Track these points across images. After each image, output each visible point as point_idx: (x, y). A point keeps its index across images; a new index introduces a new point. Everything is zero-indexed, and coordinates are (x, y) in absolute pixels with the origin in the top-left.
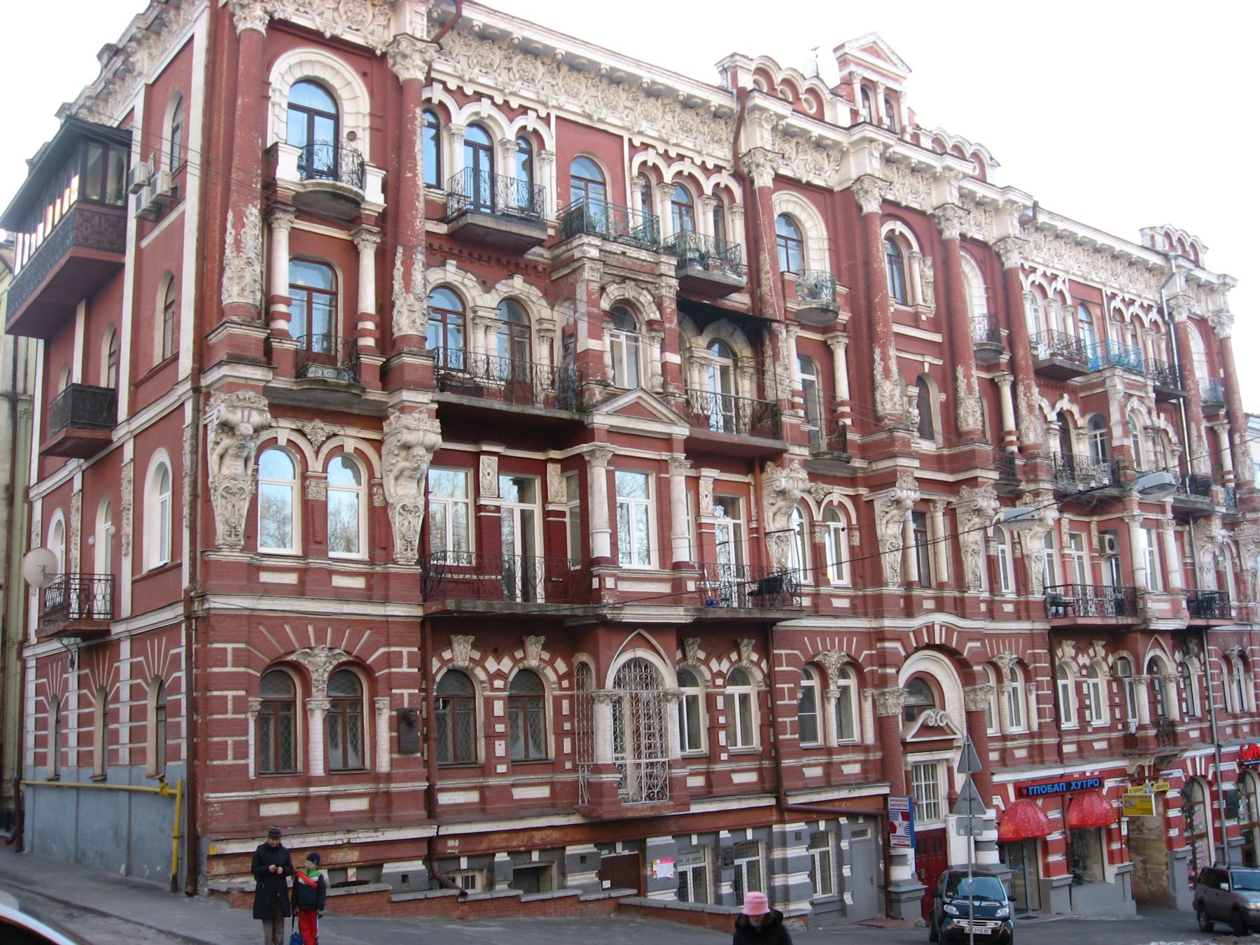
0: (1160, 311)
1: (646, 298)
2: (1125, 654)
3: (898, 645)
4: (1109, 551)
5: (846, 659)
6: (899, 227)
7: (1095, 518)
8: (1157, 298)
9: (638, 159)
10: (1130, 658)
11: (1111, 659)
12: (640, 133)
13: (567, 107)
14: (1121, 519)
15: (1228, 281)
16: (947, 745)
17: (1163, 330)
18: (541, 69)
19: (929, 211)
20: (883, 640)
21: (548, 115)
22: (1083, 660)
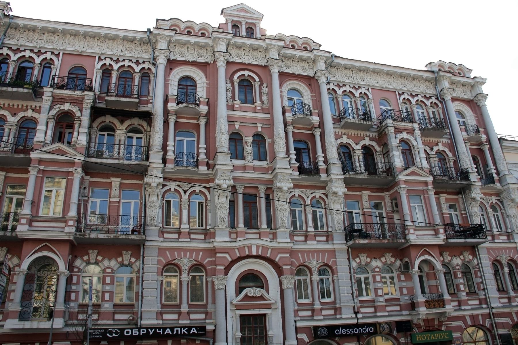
0: (437, 99)
1: (75, 109)
2: (406, 259)
3: (227, 255)
4: (395, 208)
5: (195, 262)
6: (246, 73)
7: (387, 193)
8: (435, 93)
10: (409, 261)
11: (398, 263)
12: (102, 54)
13: (67, 49)
14: (396, 191)
15: (477, 80)
16: (269, 306)
17: (440, 105)
18: (57, 38)
19: (266, 64)
20: (216, 253)
21: (59, 53)
22: (376, 263)
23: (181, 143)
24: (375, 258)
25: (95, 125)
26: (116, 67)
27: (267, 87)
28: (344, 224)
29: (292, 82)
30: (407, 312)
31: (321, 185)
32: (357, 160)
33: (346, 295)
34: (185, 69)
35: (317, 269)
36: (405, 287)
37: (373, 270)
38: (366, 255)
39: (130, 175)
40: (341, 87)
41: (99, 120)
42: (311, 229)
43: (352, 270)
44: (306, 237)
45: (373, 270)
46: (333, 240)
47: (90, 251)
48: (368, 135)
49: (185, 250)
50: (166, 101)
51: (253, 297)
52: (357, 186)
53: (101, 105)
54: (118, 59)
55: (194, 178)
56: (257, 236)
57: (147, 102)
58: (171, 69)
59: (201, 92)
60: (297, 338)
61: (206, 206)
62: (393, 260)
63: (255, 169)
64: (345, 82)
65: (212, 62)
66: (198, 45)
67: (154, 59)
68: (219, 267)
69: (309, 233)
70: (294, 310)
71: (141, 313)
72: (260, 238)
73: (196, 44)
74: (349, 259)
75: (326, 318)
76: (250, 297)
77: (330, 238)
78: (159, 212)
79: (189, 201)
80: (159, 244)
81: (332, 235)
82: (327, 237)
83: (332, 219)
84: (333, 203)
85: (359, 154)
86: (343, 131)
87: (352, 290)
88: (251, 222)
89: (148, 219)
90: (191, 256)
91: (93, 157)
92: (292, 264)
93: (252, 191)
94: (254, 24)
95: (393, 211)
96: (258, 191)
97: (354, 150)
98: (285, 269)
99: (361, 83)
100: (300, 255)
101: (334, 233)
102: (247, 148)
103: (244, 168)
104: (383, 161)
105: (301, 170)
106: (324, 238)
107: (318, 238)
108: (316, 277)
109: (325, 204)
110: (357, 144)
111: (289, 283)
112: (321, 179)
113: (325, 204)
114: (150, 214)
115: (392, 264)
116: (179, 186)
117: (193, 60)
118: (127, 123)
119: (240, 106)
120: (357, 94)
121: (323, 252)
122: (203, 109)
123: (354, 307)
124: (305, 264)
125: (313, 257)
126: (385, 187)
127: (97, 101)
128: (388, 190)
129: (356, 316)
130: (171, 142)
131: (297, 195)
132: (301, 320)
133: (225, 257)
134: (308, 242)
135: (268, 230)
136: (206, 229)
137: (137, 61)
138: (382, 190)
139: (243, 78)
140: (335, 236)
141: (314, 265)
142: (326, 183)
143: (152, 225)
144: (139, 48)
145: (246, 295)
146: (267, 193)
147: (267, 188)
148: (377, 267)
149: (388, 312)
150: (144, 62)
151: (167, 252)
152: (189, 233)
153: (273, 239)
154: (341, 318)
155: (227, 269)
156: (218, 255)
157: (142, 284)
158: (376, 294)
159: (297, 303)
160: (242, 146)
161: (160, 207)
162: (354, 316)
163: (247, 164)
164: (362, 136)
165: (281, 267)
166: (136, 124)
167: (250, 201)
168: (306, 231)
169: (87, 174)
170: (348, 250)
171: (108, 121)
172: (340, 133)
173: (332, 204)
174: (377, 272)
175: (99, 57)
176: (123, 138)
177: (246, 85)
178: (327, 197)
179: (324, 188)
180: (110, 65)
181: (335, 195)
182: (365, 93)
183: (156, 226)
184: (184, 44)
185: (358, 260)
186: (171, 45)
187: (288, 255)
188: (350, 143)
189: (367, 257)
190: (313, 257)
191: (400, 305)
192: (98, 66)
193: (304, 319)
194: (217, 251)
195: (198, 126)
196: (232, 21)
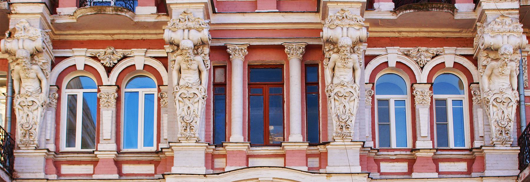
28: (519, 127)
31: (464, 35)
44: (412, 162)
46: (483, 169)
55: (131, 37)
61: (159, 99)
69: (418, 154)
77: (475, 166)
78: (44, 117)
79: (119, 90)
81: (483, 158)
82: (471, 162)
83: (486, 116)
84: (490, 77)
88: (264, 130)
89: (19, 132)
93: (270, 58)
96: (285, 56)
101: (487, 151)
106: (463, 166)
107: (444, 167)
109: (471, 81)
112: (457, 17)
114: (24, 121)
116: (95, 58)
134: (414, 175)
135: (305, 146)
136: (157, 152)
140: (489, 161)
142: (470, 25)
143: (27, 145)
146: (309, 61)
147: (309, 48)
152: (118, 164)
153: (320, 167)
161: (46, 106)
167: (266, 81)
168: (414, 150)
173: (485, 79)
178: (476, 65)
179: (468, 42)
181: (492, 56)
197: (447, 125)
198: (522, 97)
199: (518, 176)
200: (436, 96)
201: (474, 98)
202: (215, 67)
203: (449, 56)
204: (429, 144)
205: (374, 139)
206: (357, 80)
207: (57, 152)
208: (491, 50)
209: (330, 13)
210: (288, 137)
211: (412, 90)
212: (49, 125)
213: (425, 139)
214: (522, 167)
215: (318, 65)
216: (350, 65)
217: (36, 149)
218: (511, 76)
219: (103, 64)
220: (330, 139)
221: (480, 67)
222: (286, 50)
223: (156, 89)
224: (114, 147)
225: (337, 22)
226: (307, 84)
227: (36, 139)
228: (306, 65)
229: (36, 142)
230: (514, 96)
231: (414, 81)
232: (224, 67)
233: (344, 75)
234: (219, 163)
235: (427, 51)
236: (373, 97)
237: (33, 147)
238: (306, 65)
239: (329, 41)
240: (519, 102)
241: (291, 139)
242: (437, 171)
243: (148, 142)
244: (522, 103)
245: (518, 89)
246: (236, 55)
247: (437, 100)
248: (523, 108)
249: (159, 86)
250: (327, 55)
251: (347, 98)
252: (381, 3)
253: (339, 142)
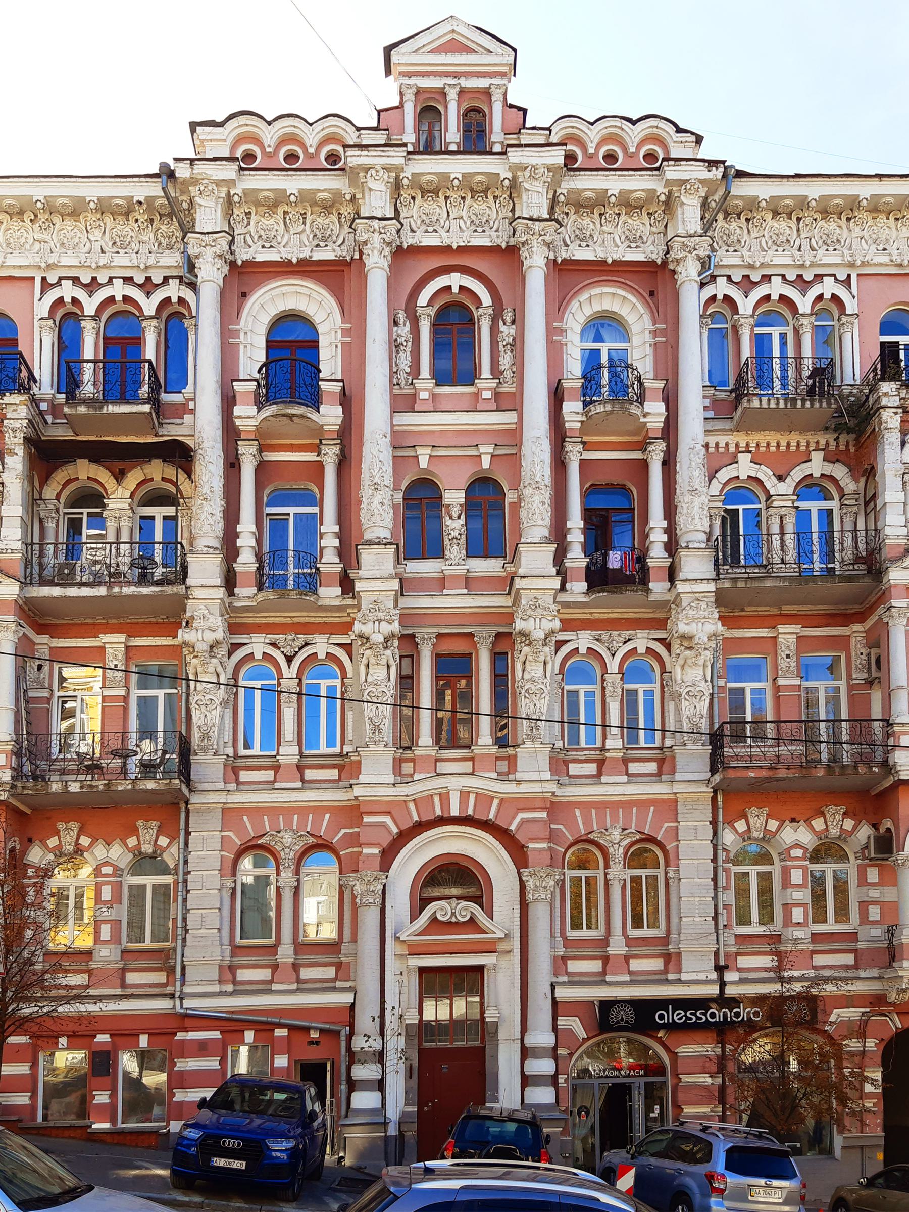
9: (52, 296)
22: (798, 836)
23: (280, 522)
24: (793, 820)
25: (49, 492)
26: (90, 306)
27: (513, 322)
28: (712, 724)
29: (596, 291)
30: (875, 972)
31: (657, 615)
32: (775, 529)
33: (698, 919)
34: (284, 289)
35: (621, 851)
36: (875, 903)
37: (785, 855)
38: (766, 810)
39: (150, 623)
40: (756, 284)
41: (61, 476)
42: (614, 743)
43: (722, 856)
45: (785, 855)
46: (673, 772)
47: (61, 826)
48: (822, 443)
49: (288, 811)
50: (228, 401)
51: (449, 923)
52: (763, 610)
53: (61, 433)
54: (94, 279)
55: (312, 620)
56: (467, 766)
57: (183, 410)
58: (244, 295)
59: (330, 363)
60: (555, 1029)
62: (849, 824)
63: (469, 582)
64: (769, 266)
65: (357, 256)
66: (314, 203)
67: (191, 267)
68: (366, 851)
69: (608, 755)
70: (555, 958)
71: (183, 968)
72: (472, 774)
73: (307, 198)
74: (714, 823)
75: (637, 979)
76: (443, 922)
80: (222, 798)
83: (678, 710)
85: (783, 511)
86: (742, 439)
87: (716, 906)
89: (196, 736)
90: (303, 822)
91: (51, 583)
92: (552, 837)
93: (459, 647)
94: (487, 93)
95: (870, 683)
97: (769, 497)
98: (534, 849)
99: (826, 260)
100: (578, 812)
102: (449, 522)
103: (441, 583)
104: (861, 525)
105: (599, 578)
108: (619, 872)
110: (781, 478)
111: (542, 885)
113: (663, 671)
114: (201, 722)
115: (845, 835)
117: (302, 256)
118: (134, 478)
119: (434, 396)
120: (804, 304)
121: (643, 804)
122: (330, 415)
123: (716, 954)
124: (591, 836)
125: (614, 818)
126: (856, 608)
127: (49, 418)
128: (860, 617)
129: (721, 977)
130: (247, 525)
131: (583, 650)
132: (571, 983)
133: (383, 825)
137: (148, 279)
138: (845, 619)
139: (444, 299)
140: (680, 762)
141: (617, 841)
143: (205, 750)
144: (148, 236)
145: (434, 920)
146: (498, 650)
148: (797, 846)
149: (815, 968)
150: (166, 279)
151: (245, 818)
153: (509, 773)
154: (679, 981)
155: (388, 856)
156: (366, 819)
157: (185, 900)
158: (788, 921)
159: (565, 939)
160: (440, 517)
162: (714, 976)
163: (450, 570)
164: (803, 449)
165: (523, 846)
166: (157, 478)
169: (41, 629)
170: (714, 799)
171: (83, 476)
172: (732, 449)
174: (797, 859)
175: (44, 279)
176: (125, 524)
177: (454, 325)
178: (669, 651)
179: (662, 624)
180: (75, 301)
182: (835, 298)
183: (215, 754)
184: (274, 203)
185: (741, 826)
186: (236, 211)
187: (544, 814)
188: (761, 476)
189: (769, 816)
190: (614, 818)
191: (855, 951)
192: (43, 308)
193: (577, 981)
194: (362, 809)
195: (319, 467)
196: (419, 92)
197: (637, 719)
198: (716, 688)
199: (709, 780)
200: (626, 686)
201: (666, 689)
202: (401, 657)
203: (642, 641)
204: (618, 744)
205: (563, 739)
206: (548, 675)
207: (236, 757)
208: (686, 637)
209: (523, 602)
210: (477, 738)
211: (603, 680)
212: (227, 725)
213: (615, 737)
214: (713, 770)
215: (507, 653)
216: (542, 659)
217: (215, 754)
218: (704, 666)
219: (283, 652)
220: (519, 741)
221: (673, 655)
222: (476, 639)
223: (339, 681)
224: (296, 750)
225: (529, 612)
226: (496, 676)
227: (215, 743)
228: (495, 654)
229: (215, 747)
230: (706, 688)
231: (605, 671)
232: (412, 656)
233: (535, 670)
234: (407, 768)
235: (619, 635)
236: (563, 689)
237: (211, 752)
238: (495, 654)
239: (522, 634)
240: (712, 695)
241: (480, 742)
242: (627, 774)
243: (330, 743)
244: (715, 696)
245: (712, 681)
246: (425, 645)
247: (627, 690)
248: (716, 700)
249: (342, 679)
250: (517, 647)
251: (538, 696)
252: (574, 583)
253: (529, 744)
